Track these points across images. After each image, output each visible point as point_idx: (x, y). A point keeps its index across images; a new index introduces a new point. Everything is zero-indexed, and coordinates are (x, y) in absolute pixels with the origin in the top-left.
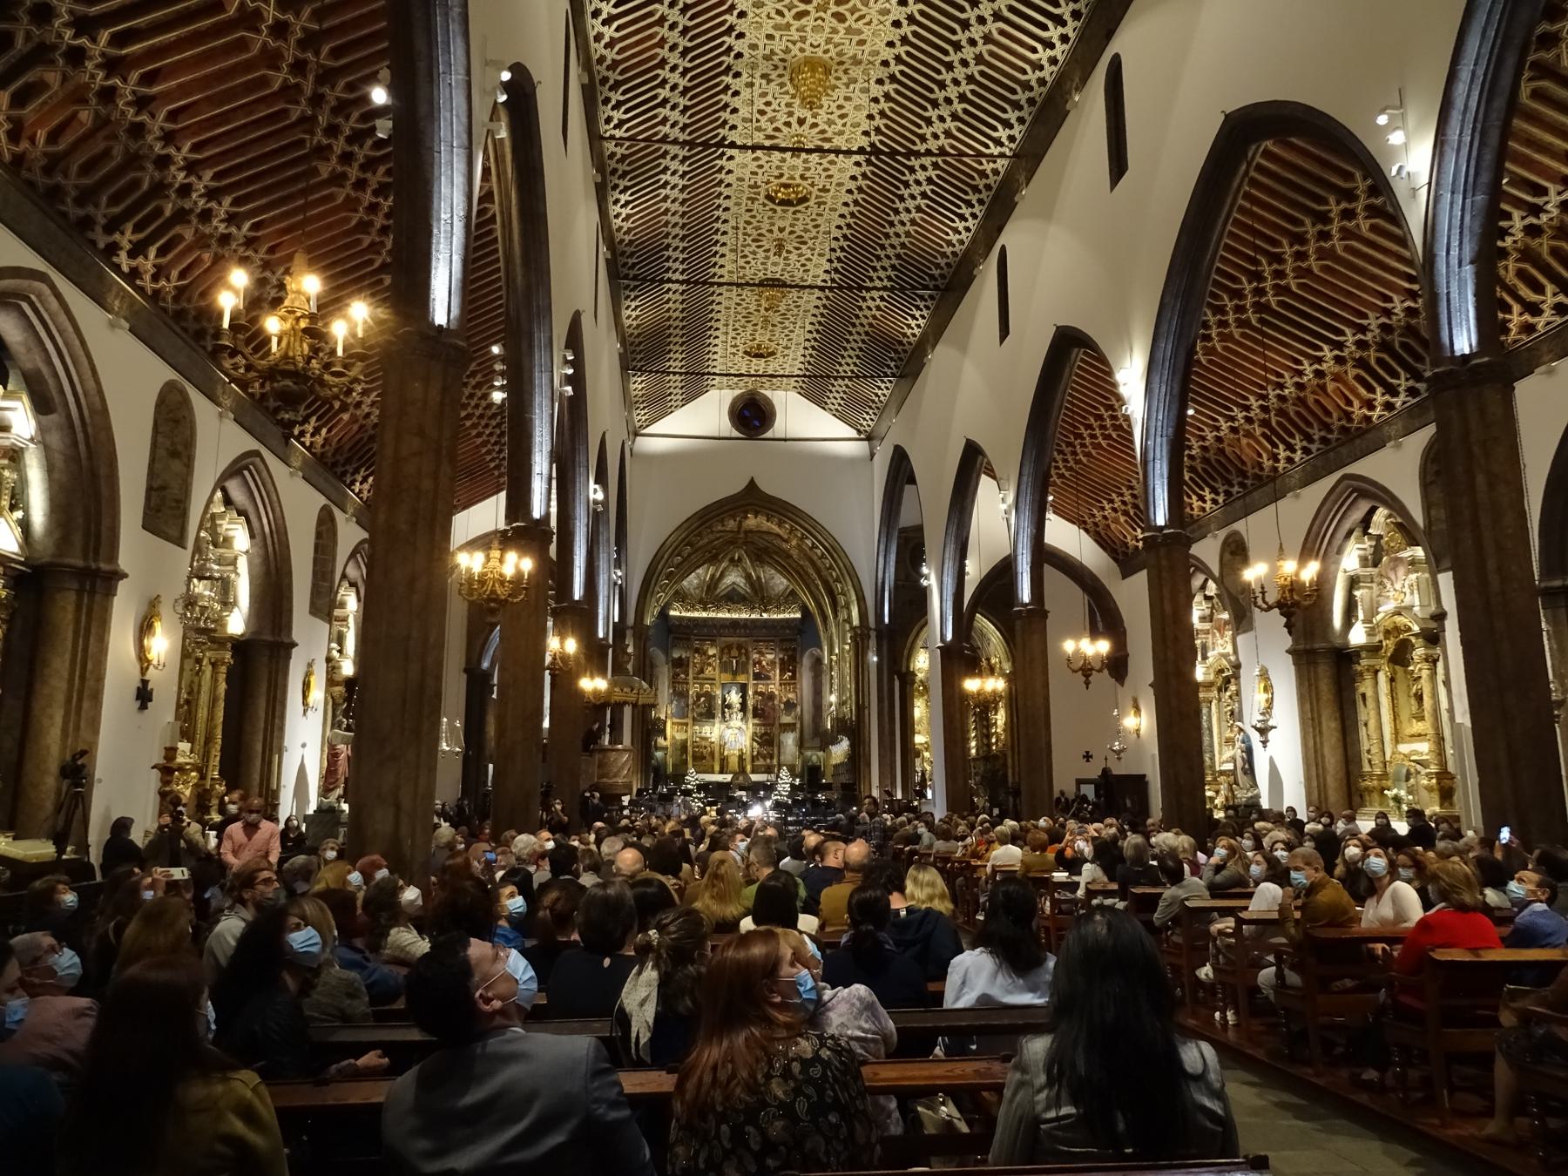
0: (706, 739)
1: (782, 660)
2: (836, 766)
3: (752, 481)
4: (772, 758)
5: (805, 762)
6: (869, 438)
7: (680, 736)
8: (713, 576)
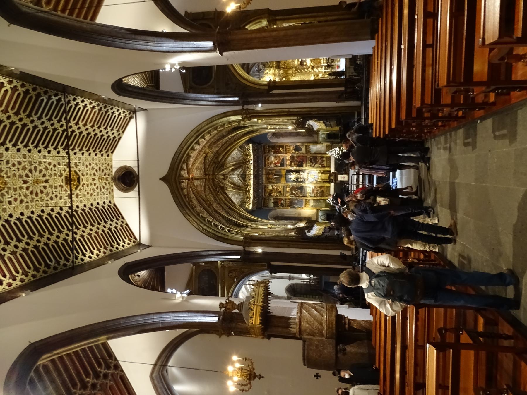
0: (313, 190)
1: (274, 153)
2: (326, 126)
3: (164, 179)
4: (323, 157)
5: (325, 141)
6: (135, 112)
7: (312, 203)
8: (233, 188)
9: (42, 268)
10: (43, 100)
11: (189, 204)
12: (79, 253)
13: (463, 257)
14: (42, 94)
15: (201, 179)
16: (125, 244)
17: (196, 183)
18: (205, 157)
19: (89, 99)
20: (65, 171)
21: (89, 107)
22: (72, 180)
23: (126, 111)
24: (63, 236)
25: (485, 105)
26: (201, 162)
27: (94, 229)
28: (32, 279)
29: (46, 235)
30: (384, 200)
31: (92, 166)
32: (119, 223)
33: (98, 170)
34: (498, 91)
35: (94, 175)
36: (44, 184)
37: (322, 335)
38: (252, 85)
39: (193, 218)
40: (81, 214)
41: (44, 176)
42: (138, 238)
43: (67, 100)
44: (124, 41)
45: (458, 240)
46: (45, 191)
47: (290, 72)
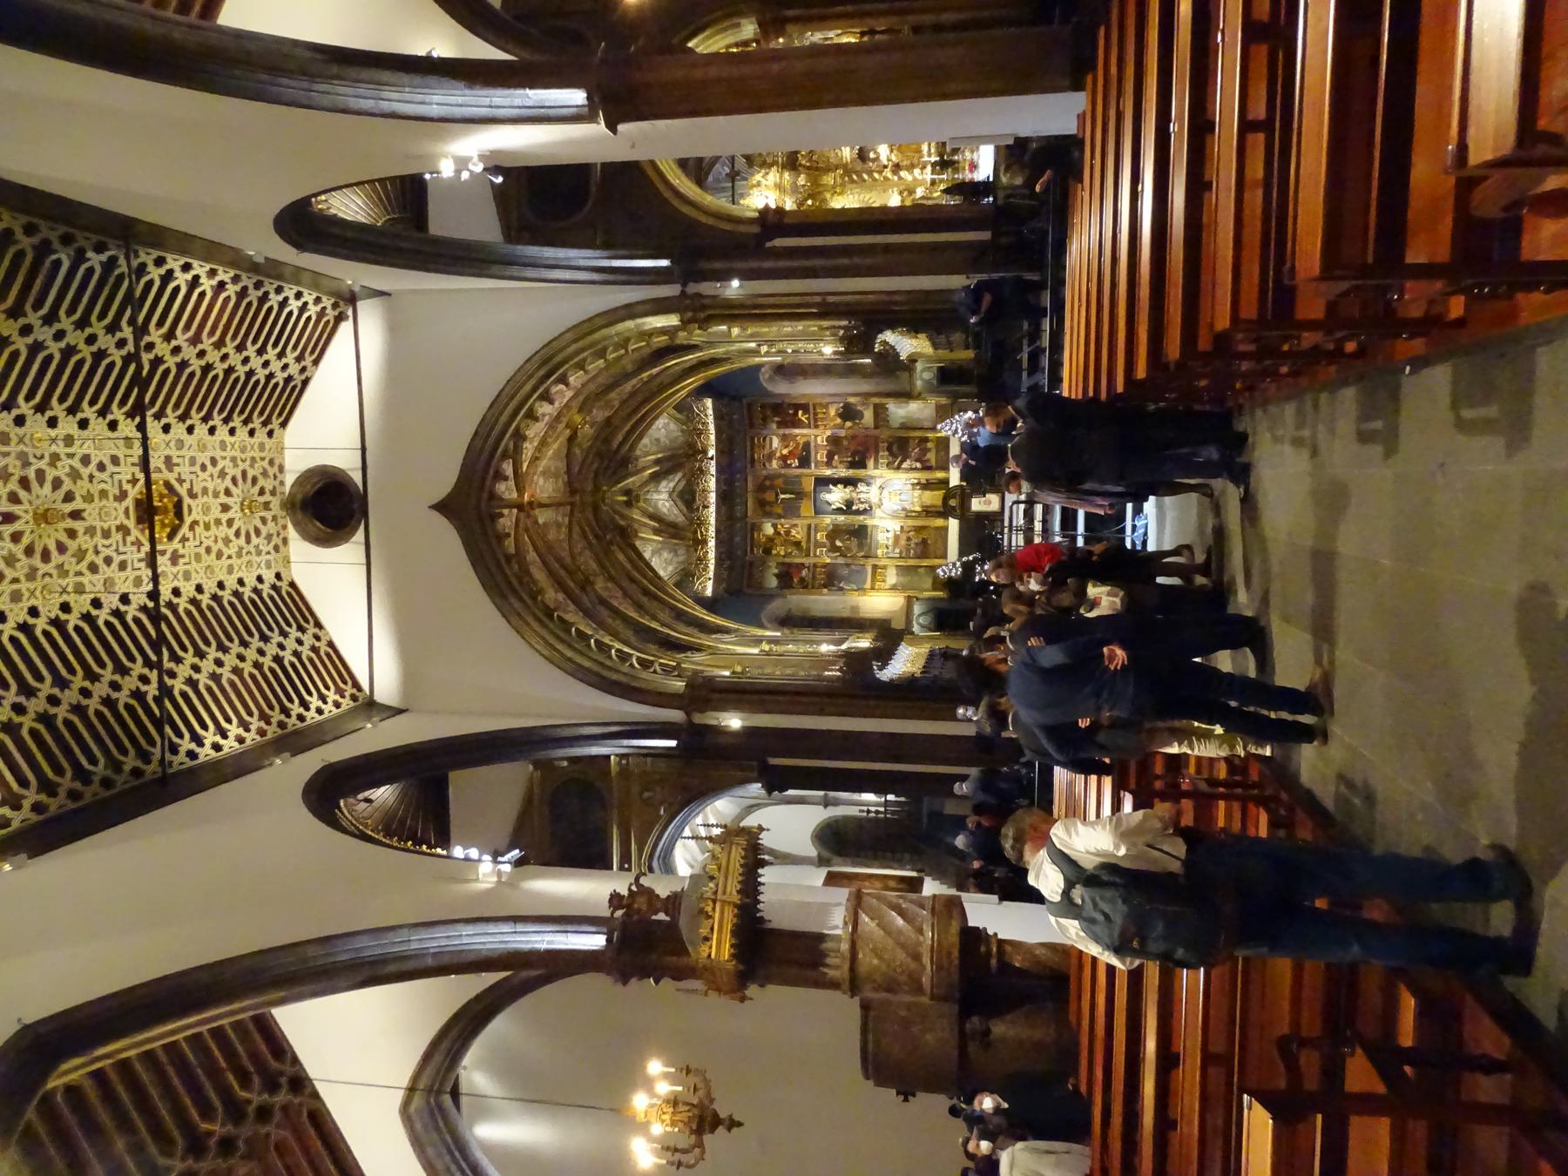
0: (897, 538)
1: (781, 425)
2: (935, 346)
3: (442, 507)
4: (926, 440)
5: (932, 389)
6: (352, 299)
7: (892, 577)
8: (657, 532)
9: (67, 782)
10: (58, 263)
11: (521, 583)
12: (180, 736)
13: (1350, 785)
14: (56, 245)
15: (559, 505)
16: (324, 706)
17: (543, 517)
18: (571, 440)
19: (206, 260)
20: (134, 481)
21: (207, 284)
22: (156, 511)
23: (324, 299)
24: (130, 683)
25: (1432, 324)
26: (556, 455)
27: (230, 660)
28: (34, 818)
29: (79, 681)
30: (1109, 594)
31: (219, 467)
32: (308, 639)
33: (239, 477)
34: (1481, 290)
35: (228, 493)
36: (70, 523)
37: (919, 989)
38: (711, 221)
39: (535, 625)
40: (189, 613)
41: (69, 497)
42: (366, 687)
43: (135, 263)
44: (305, 85)
45: (1335, 729)
46: (72, 545)
47: (829, 179)
